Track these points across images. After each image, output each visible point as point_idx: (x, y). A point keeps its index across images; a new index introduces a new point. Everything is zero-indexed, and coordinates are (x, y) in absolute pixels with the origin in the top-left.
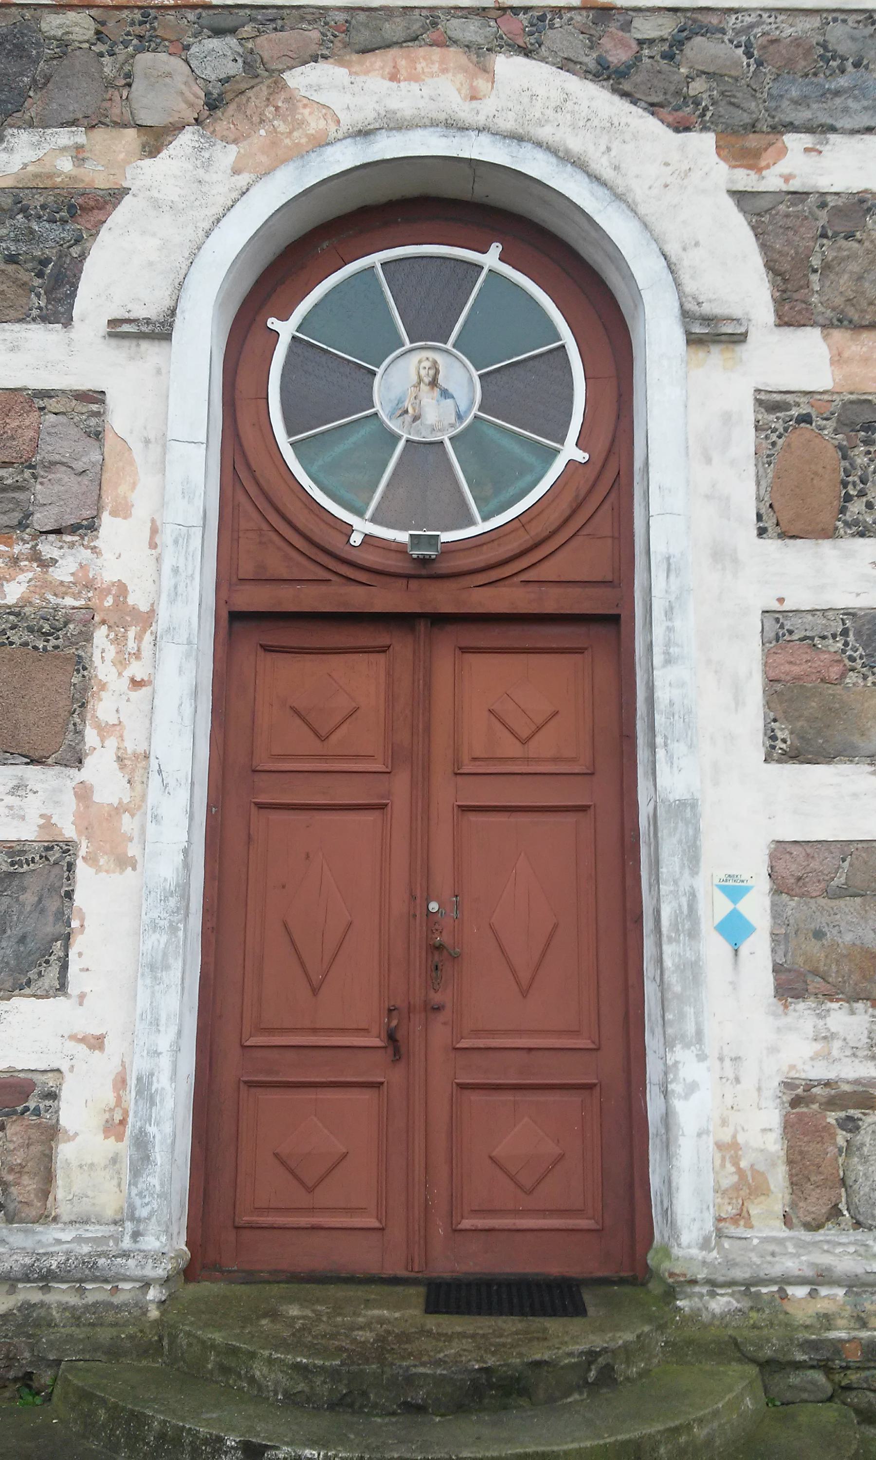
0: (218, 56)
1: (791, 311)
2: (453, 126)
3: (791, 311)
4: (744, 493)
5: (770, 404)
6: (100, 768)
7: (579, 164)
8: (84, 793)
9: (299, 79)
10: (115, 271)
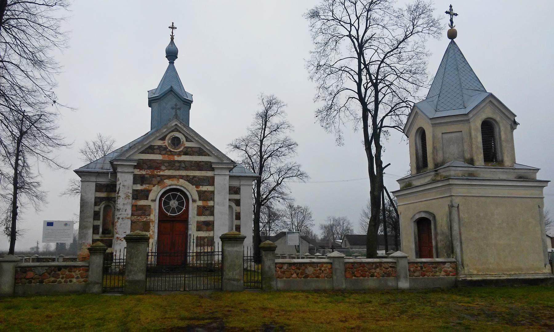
0: (159, 179)
1: (199, 200)
2: (176, 185)
3: (199, 200)
4: (196, 212)
5: (198, 206)
6: (151, 232)
7: (185, 188)
9: (165, 181)
10: (151, 196)
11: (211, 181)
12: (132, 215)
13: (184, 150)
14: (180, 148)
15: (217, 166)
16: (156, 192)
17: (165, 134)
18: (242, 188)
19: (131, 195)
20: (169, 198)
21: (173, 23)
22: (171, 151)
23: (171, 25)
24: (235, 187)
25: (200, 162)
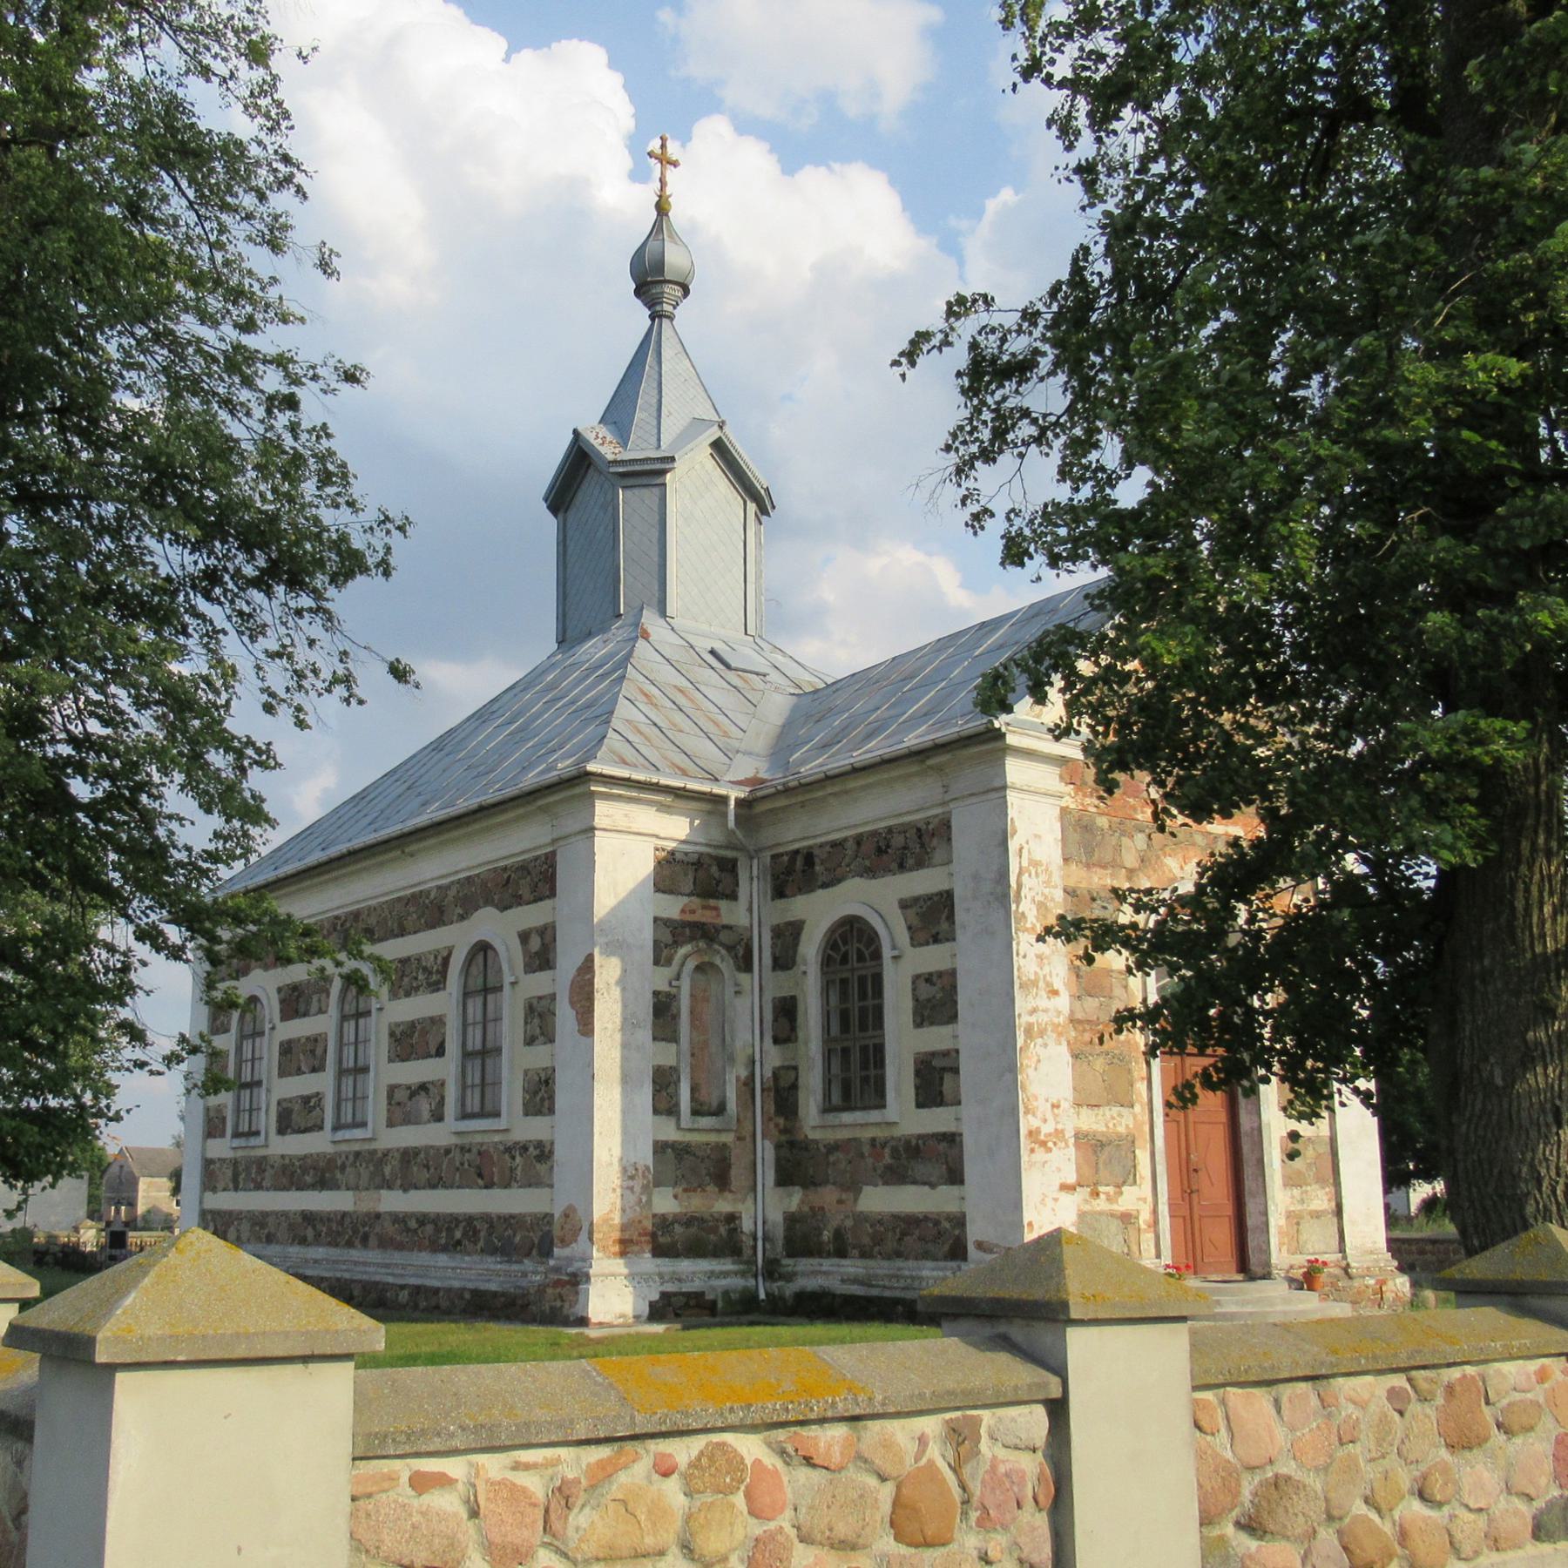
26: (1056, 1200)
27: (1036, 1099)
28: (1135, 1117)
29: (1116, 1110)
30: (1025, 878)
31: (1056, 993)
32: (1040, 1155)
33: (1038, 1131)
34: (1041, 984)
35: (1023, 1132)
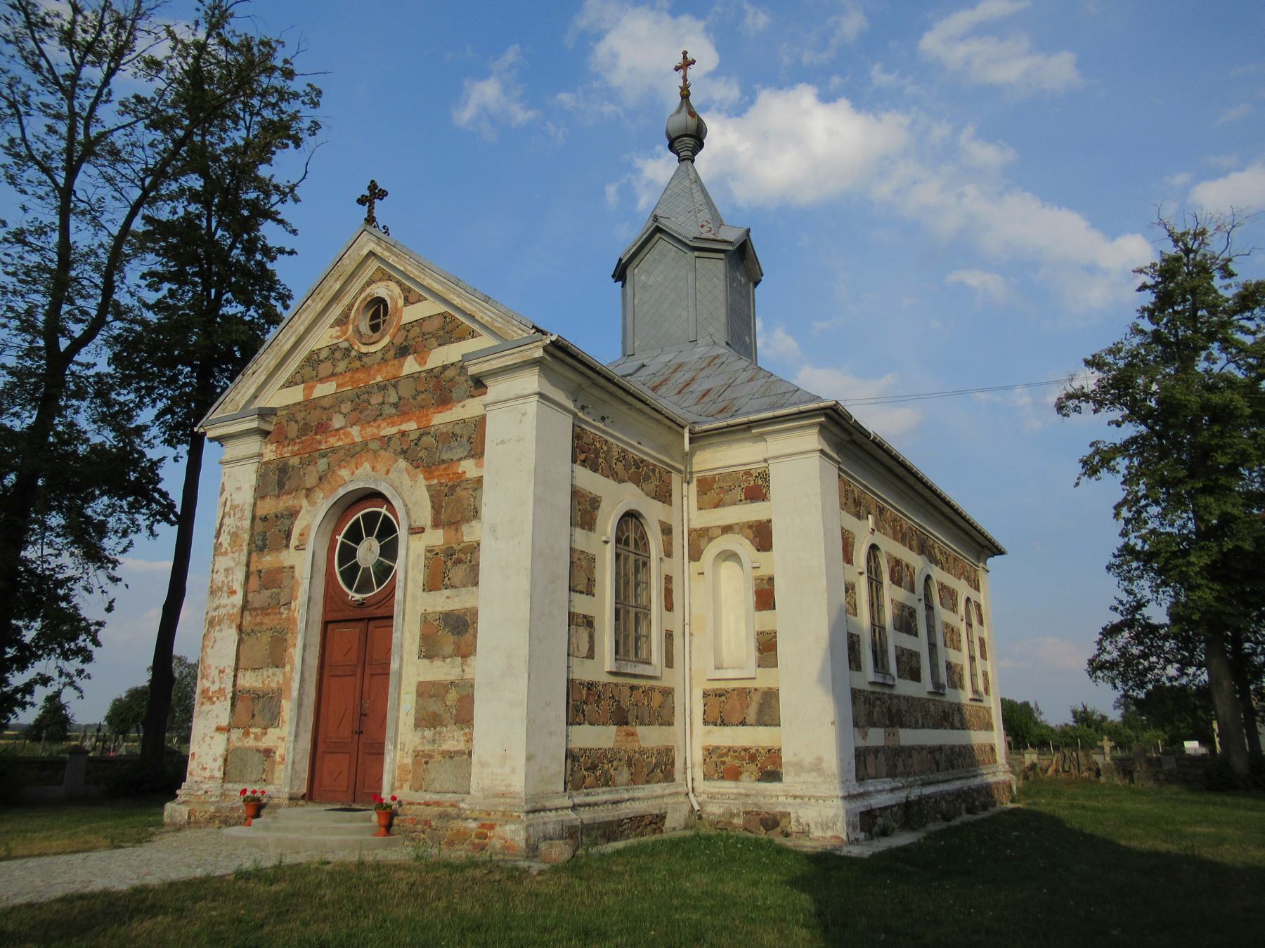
4: (420, 579)
6: (288, 668)
8: (284, 674)
11: (473, 438)
12: (245, 607)
13: (399, 340)
14: (383, 337)
15: (485, 367)
16: (312, 517)
17: (346, 300)
18: (775, 471)
19: (246, 536)
20: (355, 535)
21: (685, 53)
22: (361, 356)
23: (679, 60)
24: (748, 473)
25: (445, 367)
26: (212, 738)
27: (209, 667)
28: (284, 674)
29: (271, 671)
30: (227, 521)
31: (234, 592)
32: (207, 707)
33: (208, 689)
34: (225, 588)
35: (198, 690)
